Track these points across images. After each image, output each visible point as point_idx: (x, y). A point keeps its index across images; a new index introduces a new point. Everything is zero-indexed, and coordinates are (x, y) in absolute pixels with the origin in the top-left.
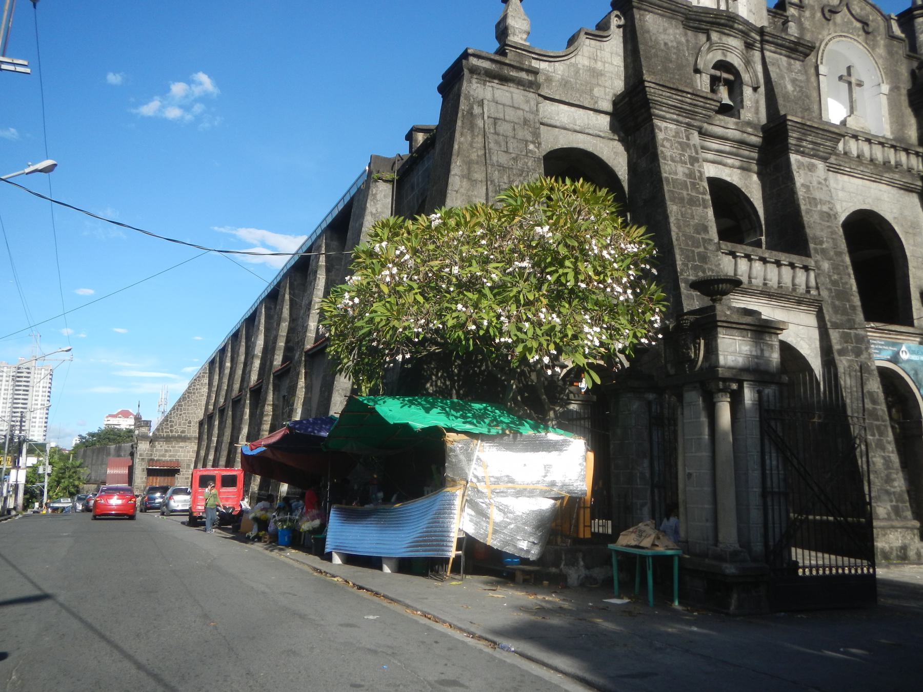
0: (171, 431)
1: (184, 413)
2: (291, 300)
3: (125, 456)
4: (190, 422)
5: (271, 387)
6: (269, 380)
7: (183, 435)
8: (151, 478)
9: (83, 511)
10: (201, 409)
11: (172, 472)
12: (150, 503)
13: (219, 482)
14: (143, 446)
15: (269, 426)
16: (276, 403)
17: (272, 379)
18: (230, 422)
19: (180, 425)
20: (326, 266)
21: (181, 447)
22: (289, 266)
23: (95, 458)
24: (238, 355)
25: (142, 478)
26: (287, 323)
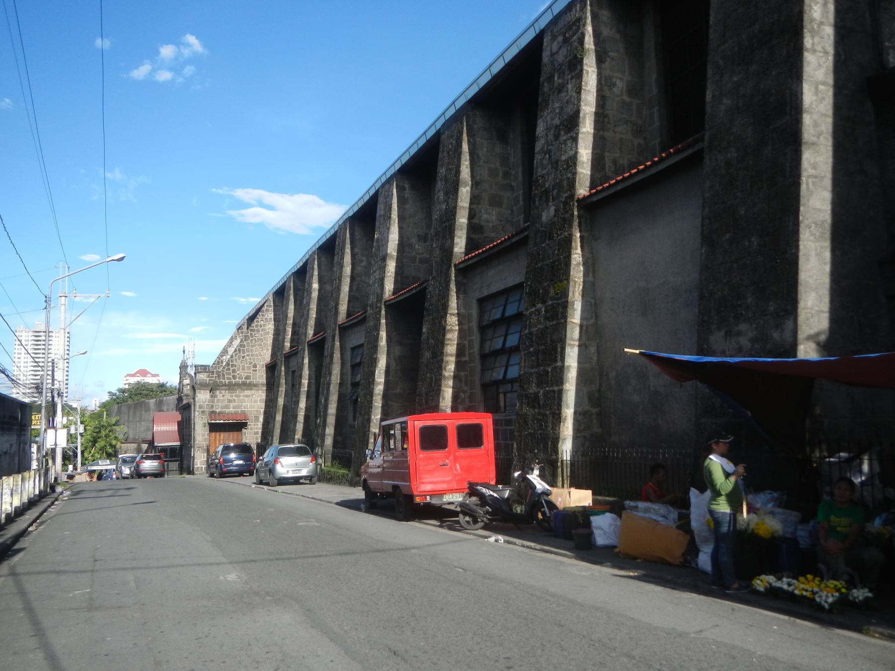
0: (234, 377)
1: (247, 355)
2: (472, 153)
3: (168, 410)
4: (255, 366)
5: (453, 287)
6: (448, 277)
7: (248, 381)
8: (213, 434)
9: (132, 476)
10: (267, 350)
11: (238, 426)
12: (226, 467)
13: (452, 438)
14: (203, 396)
15: (455, 347)
16: (463, 311)
17: (453, 275)
18: (339, 355)
19: (243, 369)
20: (597, 51)
21: (247, 396)
22: (459, 104)
23: (131, 414)
24: (341, 266)
25: (204, 435)
26: (468, 188)
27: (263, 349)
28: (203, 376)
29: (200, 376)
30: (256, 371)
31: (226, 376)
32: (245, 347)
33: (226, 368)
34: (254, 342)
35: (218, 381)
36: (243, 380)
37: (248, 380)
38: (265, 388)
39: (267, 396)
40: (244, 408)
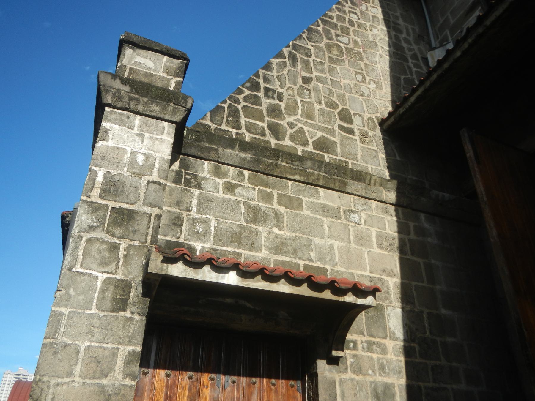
1: (318, 79)
10: (379, 85)
21: (325, 210)
27: (364, 77)
28: (150, 64)
29: (139, 59)
30: (351, 132)
31: (243, 120)
32: (310, 55)
33: (247, 92)
34: (336, 52)
35: (213, 126)
36: (310, 148)
37: (326, 155)
38: (392, 196)
39: (402, 229)
40: (321, 259)
